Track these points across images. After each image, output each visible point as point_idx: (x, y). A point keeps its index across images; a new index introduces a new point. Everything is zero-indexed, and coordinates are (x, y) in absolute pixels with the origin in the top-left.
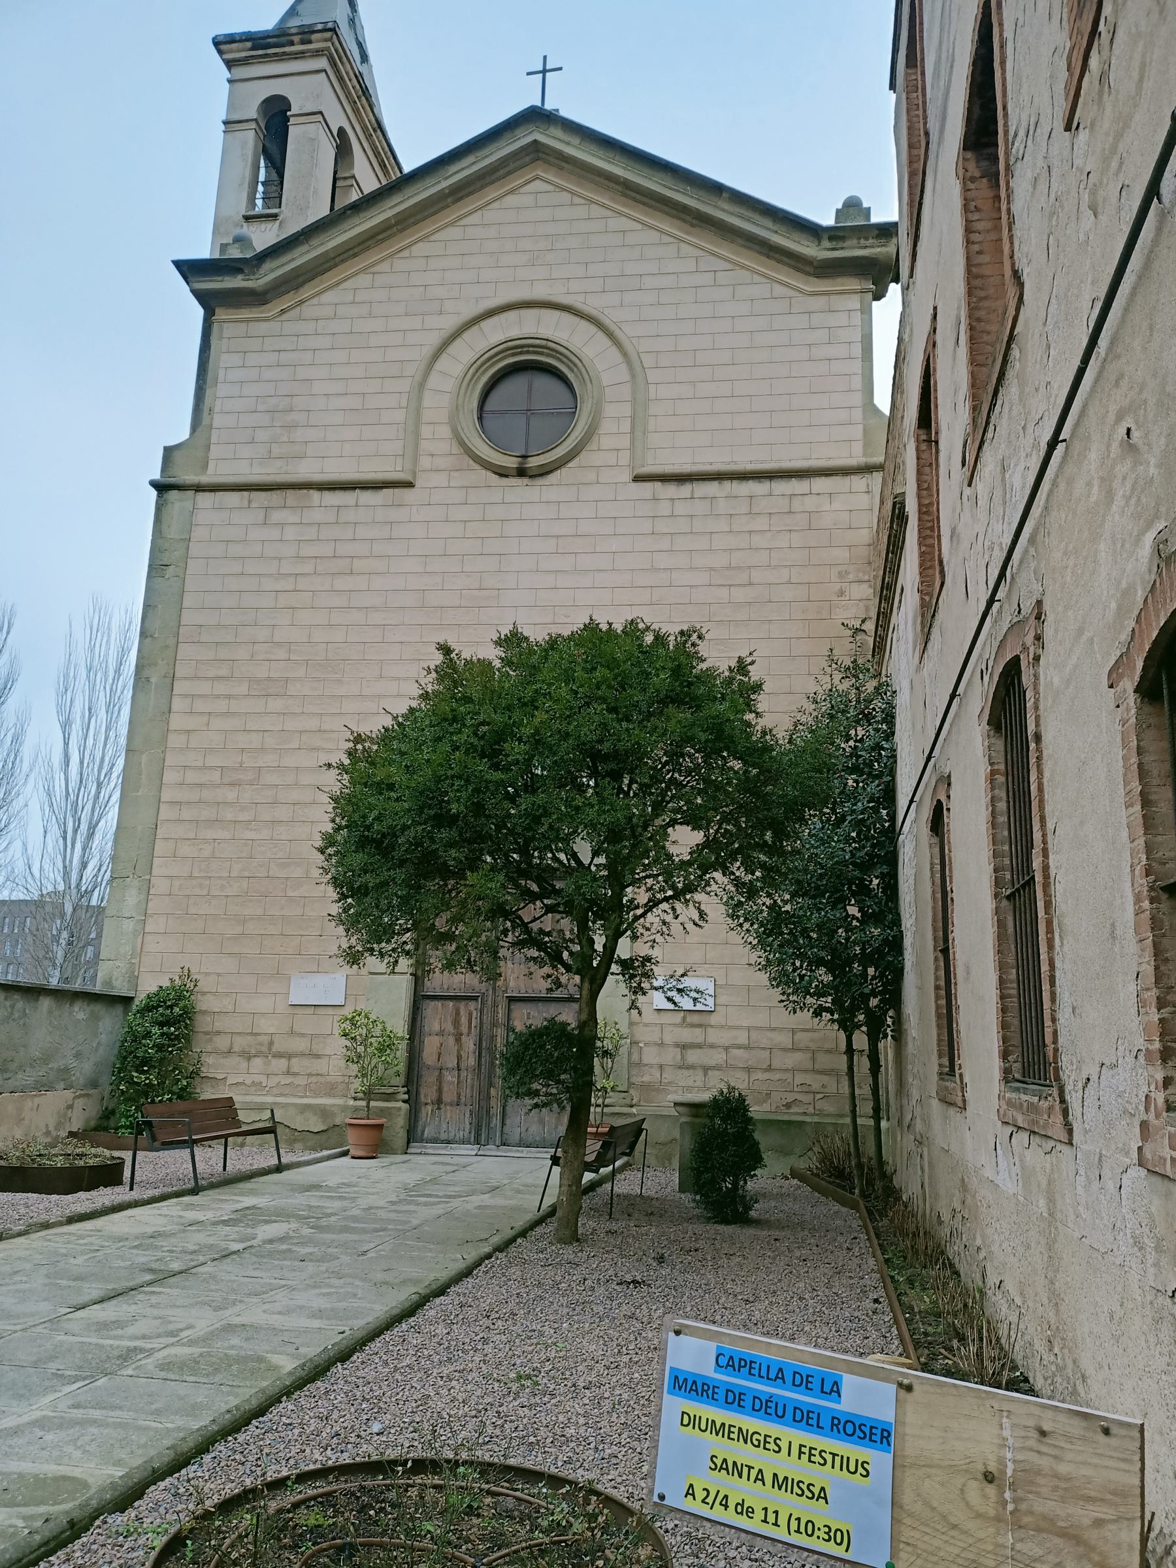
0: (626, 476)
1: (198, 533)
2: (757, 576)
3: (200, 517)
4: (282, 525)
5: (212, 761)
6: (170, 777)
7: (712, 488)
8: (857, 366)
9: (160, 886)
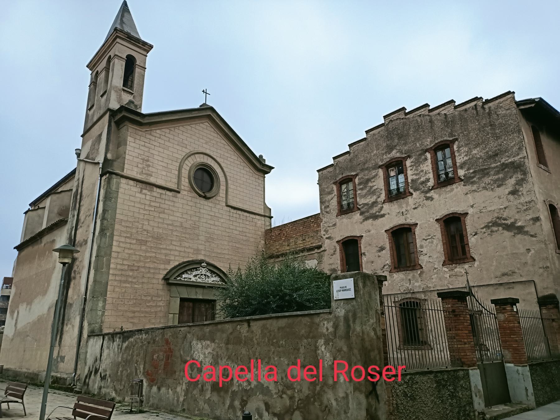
0: (224, 204)
1: (121, 190)
2: (247, 234)
3: (122, 185)
4: (146, 195)
6: (112, 266)
7: (239, 212)
8: (262, 193)
9: (109, 300)
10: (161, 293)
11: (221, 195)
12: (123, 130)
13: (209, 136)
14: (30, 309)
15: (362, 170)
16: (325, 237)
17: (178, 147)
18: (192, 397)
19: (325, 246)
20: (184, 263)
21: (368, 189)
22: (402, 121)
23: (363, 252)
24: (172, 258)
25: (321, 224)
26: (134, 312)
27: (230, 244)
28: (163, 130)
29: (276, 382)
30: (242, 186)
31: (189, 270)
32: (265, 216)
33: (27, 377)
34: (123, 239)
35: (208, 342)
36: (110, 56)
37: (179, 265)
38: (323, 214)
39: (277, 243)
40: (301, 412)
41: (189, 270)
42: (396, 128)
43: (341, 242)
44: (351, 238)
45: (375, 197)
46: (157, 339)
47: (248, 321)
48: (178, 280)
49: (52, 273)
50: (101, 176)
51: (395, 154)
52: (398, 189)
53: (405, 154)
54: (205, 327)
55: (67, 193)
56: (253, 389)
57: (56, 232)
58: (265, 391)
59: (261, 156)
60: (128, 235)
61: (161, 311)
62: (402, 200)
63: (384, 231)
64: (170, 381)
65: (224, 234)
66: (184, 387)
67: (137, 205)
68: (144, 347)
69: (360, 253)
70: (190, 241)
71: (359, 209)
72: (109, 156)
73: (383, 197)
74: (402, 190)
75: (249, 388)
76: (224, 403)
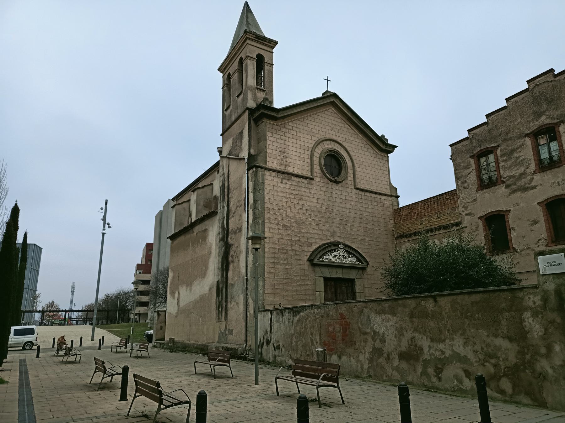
0: (353, 187)
1: (266, 182)
2: (377, 215)
4: (286, 184)
5: (276, 246)
6: (266, 250)
7: (367, 194)
8: (387, 173)
9: (267, 280)
10: (307, 273)
11: (349, 178)
12: (262, 126)
13: (334, 122)
14: (191, 290)
15: (505, 140)
16: (464, 214)
17: (308, 137)
18: (377, 364)
19: (465, 222)
20: (327, 244)
21: (513, 160)
22: (550, 84)
23: (511, 227)
24: (314, 241)
25: (459, 200)
26: (288, 291)
27: (362, 225)
28: (294, 122)
29: (475, 352)
30: (368, 168)
31: (328, 251)
32: (391, 196)
33: (196, 348)
34: (272, 226)
35: (389, 316)
36: (241, 58)
37: (320, 247)
38: (459, 190)
39: (408, 222)
40: (509, 379)
41: (328, 251)
42: (543, 92)
43: (484, 218)
44: (495, 213)
45: (523, 168)
46: (331, 313)
47: (434, 298)
48: (320, 261)
49: (209, 258)
50: (248, 170)
51: (544, 120)
52: (551, 158)
53: (558, 119)
54: (384, 303)
55: (209, 187)
56: (448, 358)
57: (206, 222)
58: (463, 360)
59: (383, 136)
60: (276, 222)
61: (309, 289)
62: (556, 169)
63: (536, 203)
64: (350, 351)
65: (356, 216)
66: (367, 356)
67: (280, 194)
68: (318, 321)
69: (508, 228)
70: (326, 224)
71: (504, 182)
72: (252, 151)
73: (533, 167)
74: (555, 158)
75: (443, 356)
76: (415, 371)
